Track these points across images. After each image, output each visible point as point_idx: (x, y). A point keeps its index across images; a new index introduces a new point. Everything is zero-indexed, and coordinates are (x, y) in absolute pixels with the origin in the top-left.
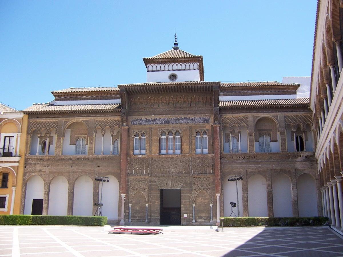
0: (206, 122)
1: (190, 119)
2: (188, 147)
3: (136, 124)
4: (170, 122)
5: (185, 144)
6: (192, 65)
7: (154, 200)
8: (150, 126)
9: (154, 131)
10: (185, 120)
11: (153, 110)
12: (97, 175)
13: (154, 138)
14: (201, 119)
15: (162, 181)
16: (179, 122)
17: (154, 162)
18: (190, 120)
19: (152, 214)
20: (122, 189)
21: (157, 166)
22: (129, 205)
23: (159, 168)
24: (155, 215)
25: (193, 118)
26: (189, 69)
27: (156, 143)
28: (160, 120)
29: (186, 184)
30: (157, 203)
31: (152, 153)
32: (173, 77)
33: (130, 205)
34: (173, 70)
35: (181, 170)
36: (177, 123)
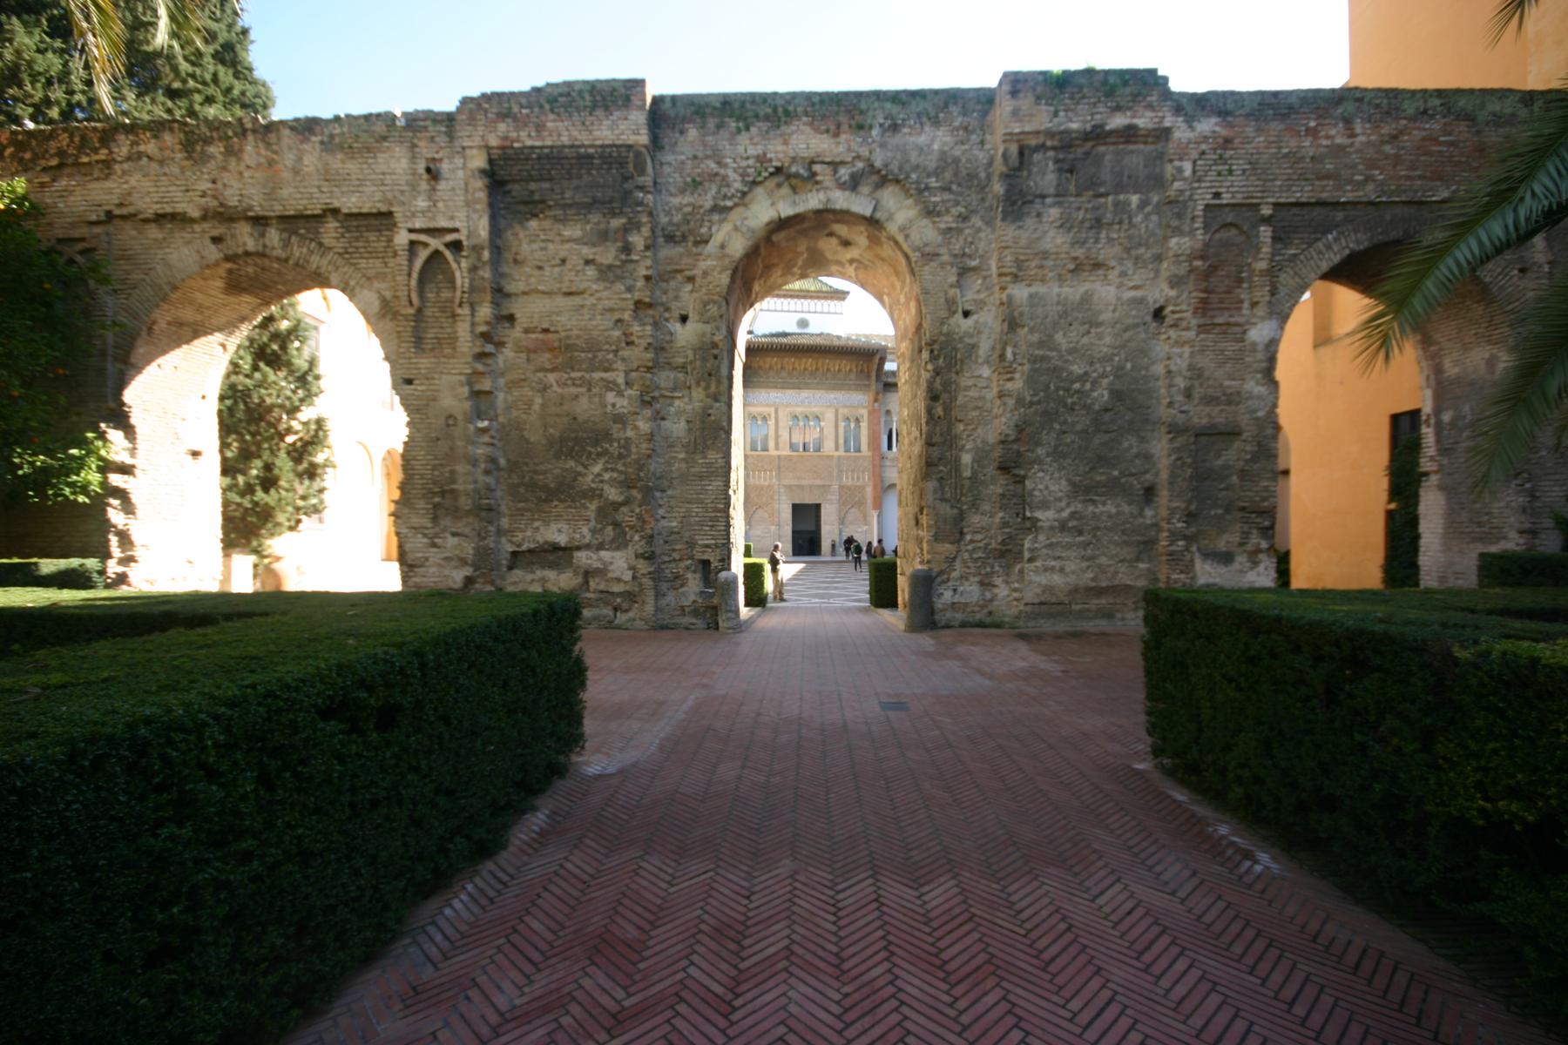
32: (803, 323)
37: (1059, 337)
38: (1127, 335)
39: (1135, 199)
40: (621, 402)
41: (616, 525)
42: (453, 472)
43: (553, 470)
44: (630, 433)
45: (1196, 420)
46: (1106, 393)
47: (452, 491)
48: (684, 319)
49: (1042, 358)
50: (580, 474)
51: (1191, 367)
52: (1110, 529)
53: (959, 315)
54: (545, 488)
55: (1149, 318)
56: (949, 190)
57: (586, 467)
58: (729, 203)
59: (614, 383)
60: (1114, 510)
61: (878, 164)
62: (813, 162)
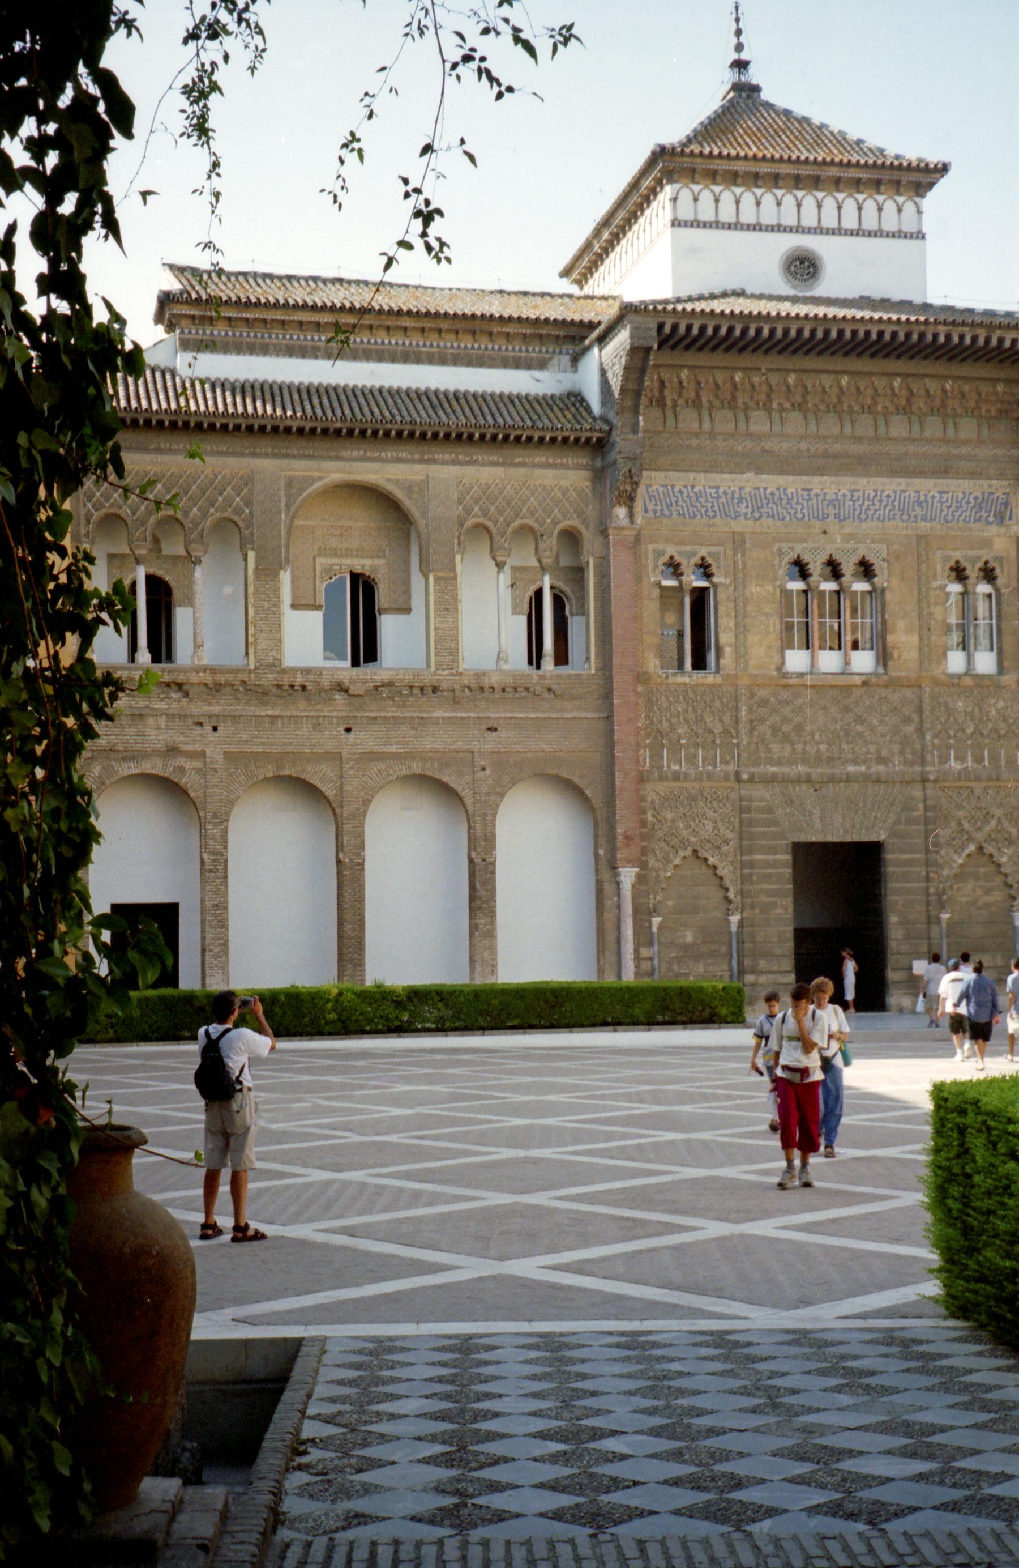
0: (991, 519)
1: (922, 498)
2: (915, 639)
3: (666, 512)
4: (831, 511)
5: (901, 624)
6: (890, 206)
7: (769, 893)
8: (740, 526)
9: (755, 553)
10: (896, 503)
11: (749, 444)
12: (488, 772)
13: (758, 589)
14: (968, 502)
15: (802, 804)
16: (870, 513)
17: (763, 711)
18: (919, 503)
19: (762, 964)
20: (627, 846)
21: (775, 730)
22: (650, 922)
23: (786, 738)
24: (775, 968)
25: (933, 497)
26: (840, 229)
27: (767, 615)
28: (781, 500)
29: (909, 822)
30: (779, 911)
31: (752, 663)
32: (803, 266)
33: (656, 921)
34: (798, 229)
35: (884, 753)
36: (863, 516)
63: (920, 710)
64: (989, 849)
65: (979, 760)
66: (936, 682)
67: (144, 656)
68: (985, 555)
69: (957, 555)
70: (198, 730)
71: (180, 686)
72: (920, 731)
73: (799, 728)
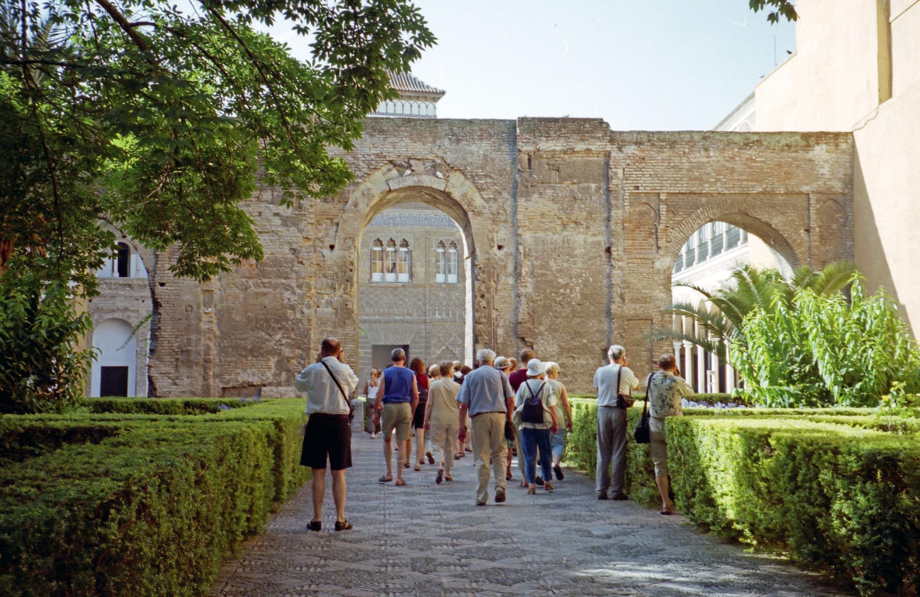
2: (423, 269)
5: (418, 264)
17: (362, 296)
21: (367, 303)
23: (372, 306)
29: (420, 338)
37: (552, 263)
38: (589, 263)
39: (593, 186)
40: (293, 298)
41: (288, 371)
42: (189, 339)
43: (250, 338)
44: (299, 316)
45: (627, 312)
46: (579, 295)
47: (187, 351)
48: (332, 247)
49: (542, 275)
50: (267, 340)
51: (623, 282)
52: (583, 374)
53: (496, 247)
54: (245, 348)
55: (603, 254)
56: (490, 177)
57: (271, 336)
58: (360, 181)
59: (289, 285)
60: (584, 363)
61: (448, 161)
62: (410, 158)
63: (425, 296)
64: (450, 348)
65: (448, 315)
66: (431, 286)
67: (116, 274)
68: (452, 238)
69: (441, 239)
70: (136, 302)
71: (130, 285)
72: (424, 304)
73: (376, 302)
